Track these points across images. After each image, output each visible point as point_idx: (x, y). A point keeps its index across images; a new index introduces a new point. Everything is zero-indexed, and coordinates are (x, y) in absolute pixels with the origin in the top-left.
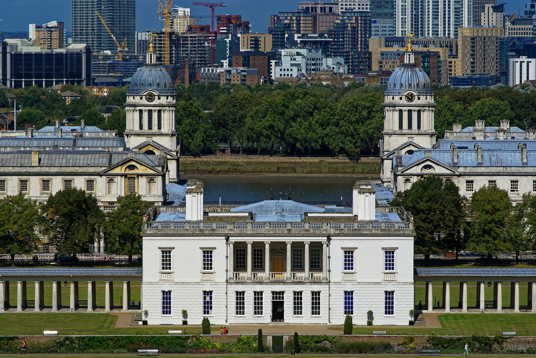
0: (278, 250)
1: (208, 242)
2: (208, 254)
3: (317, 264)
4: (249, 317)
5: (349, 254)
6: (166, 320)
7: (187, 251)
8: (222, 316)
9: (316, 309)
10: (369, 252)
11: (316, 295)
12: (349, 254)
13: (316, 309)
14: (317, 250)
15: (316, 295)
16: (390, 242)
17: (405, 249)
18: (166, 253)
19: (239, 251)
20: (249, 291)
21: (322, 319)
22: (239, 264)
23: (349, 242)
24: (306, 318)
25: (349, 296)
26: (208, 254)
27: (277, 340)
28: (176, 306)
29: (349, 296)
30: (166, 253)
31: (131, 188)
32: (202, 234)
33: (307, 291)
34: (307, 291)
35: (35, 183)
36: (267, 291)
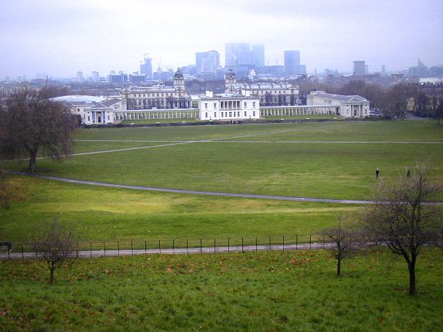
0: (230, 103)
1: (215, 102)
2: (215, 104)
3: (238, 106)
4: (224, 118)
5: (245, 104)
6: (206, 119)
7: (211, 104)
8: (218, 118)
9: (239, 115)
10: (250, 102)
11: (238, 113)
12: (245, 104)
13: (239, 115)
14: (238, 102)
15: (238, 113)
16: (254, 101)
17: (258, 102)
18: (206, 104)
19: (222, 103)
20: (224, 112)
21: (240, 118)
22: (222, 106)
23: (246, 101)
24: (237, 117)
25: (245, 112)
26: (215, 104)
27: (234, 122)
28: (209, 115)
29: (245, 112)
30: (206, 104)
31: (180, 95)
32: (214, 100)
33: (237, 112)
34: (237, 112)
35: (165, 94)
36: (228, 112)
